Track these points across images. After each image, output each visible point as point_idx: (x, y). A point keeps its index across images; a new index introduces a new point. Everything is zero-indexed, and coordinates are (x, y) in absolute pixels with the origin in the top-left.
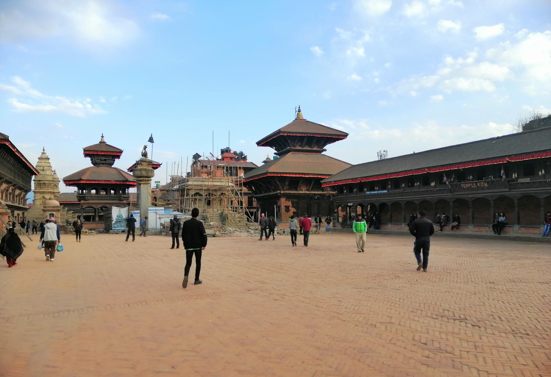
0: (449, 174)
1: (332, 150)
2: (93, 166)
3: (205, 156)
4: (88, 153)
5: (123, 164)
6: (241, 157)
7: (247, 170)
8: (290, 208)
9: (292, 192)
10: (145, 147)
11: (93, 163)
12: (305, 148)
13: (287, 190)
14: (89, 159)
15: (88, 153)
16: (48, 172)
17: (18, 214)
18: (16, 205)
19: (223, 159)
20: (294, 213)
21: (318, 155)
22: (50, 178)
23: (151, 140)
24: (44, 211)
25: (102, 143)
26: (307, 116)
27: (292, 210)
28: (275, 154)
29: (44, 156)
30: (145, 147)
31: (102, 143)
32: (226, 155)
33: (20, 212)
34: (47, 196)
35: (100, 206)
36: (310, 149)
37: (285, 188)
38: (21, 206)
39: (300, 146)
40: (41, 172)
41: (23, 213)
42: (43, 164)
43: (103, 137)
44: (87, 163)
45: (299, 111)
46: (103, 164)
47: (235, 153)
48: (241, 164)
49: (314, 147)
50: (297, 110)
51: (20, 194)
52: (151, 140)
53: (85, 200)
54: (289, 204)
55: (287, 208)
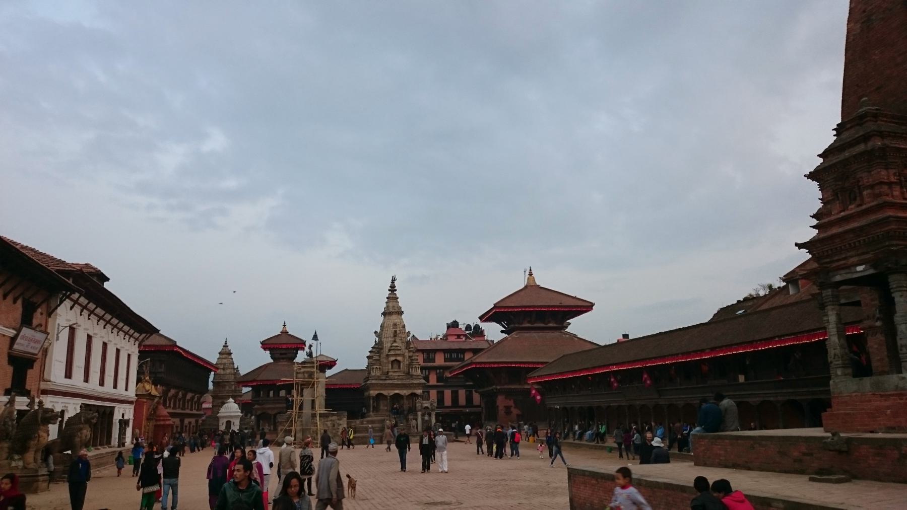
1: (577, 326)
2: (272, 361)
4: (266, 345)
6: (478, 332)
7: (476, 351)
8: (512, 409)
9: (513, 387)
10: (310, 346)
11: (272, 358)
12: (536, 325)
15: (266, 345)
17: (190, 423)
18: (188, 411)
20: (518, 415)
21: (557, 334)
25: (285, 333)
27: (515, 411)
28: (502, 332)
31: (285, 333)
32: (453, 331)
33: (193, 420)
35: (276, 411)
36: (542, 325)
38: (195, 412)
39: (529, 322)
41: (197, 421)
44: (266, 358)
45: (531, 274)
46: (283, 359)
47: (468, 327)
48: (474, 343)
50: (527, 273)
51: (193, 398)
53: (258, 404)
54: (511, 403)
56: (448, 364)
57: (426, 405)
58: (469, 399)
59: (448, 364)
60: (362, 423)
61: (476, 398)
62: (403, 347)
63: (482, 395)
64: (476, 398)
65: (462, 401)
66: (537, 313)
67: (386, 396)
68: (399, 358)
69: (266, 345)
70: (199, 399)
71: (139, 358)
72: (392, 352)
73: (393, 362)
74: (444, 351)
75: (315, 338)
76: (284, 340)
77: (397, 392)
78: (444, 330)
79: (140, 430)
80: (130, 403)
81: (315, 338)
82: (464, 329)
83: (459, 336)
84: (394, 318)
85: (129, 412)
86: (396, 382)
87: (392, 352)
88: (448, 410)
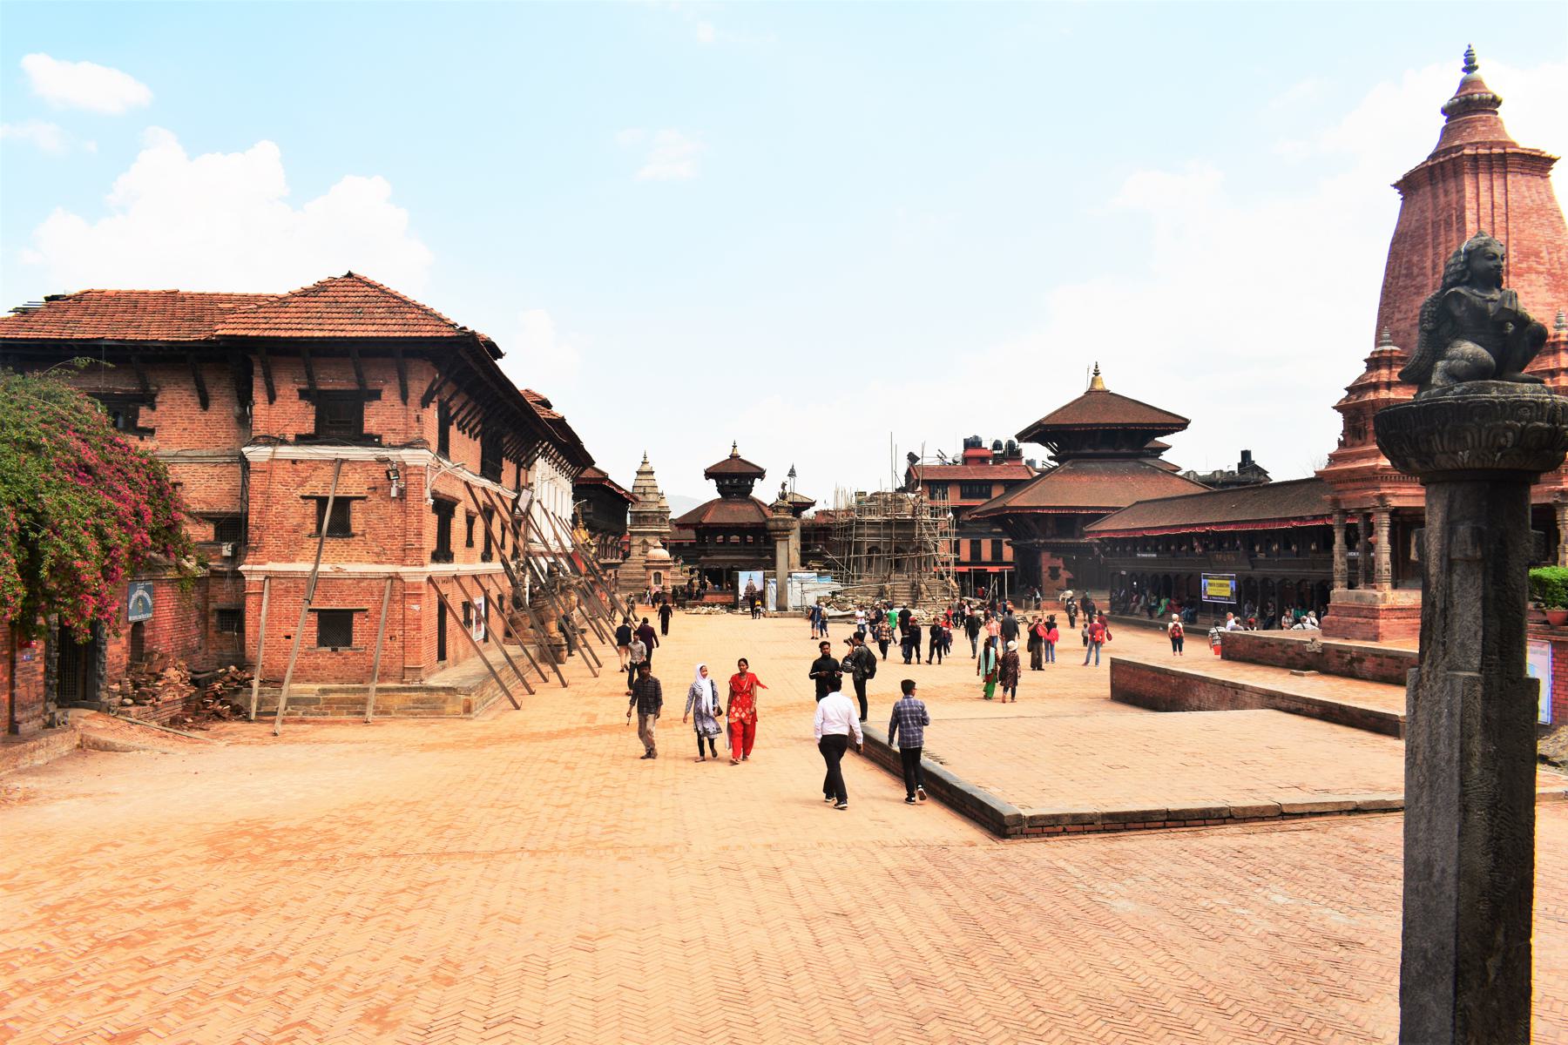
0: (1200, 536)
3: (929, 459)
5: (765, 492)
6: (1013, 453)
10: (784, 485)
13: (1053, 536)
14: (713, 482)
16: (651, 498)
18: (609, 560)
19: (966, 460)
22: (655, 508)
23: (792, 473)
24: (647, 568)
25: (734, 457)
26: (1113, 383)
27: (1065, 575)
28: (1050, 458)
29: (646, 468)
30: (784, 485)
32: (972, 452)
34: (650, 540)
35: (728, 565)
36: (1111, 451)
37: (1049, 533)
40: (641, 498)
42: (644, 483)
44: (710, 491)
45: (1097, 373)
47: (997, 445)
49: (1121, 446)
52: (792, 473)
54: (1060, 563)
55: (1054, 573)
56: (966, 502)
58: (997, 557)
59: (966, 502)
61: (1008, 553)
63: (1016, 550)
64: (1008, 553)
65: (986, 554)
66: (1107, 433)
69: (709, 474)
71: (575, 498)
74: (961, 483)
76: (736, 469)
78: (960, 450)
82: (990, 447)
83: (983, 460)
88: (965, 569)
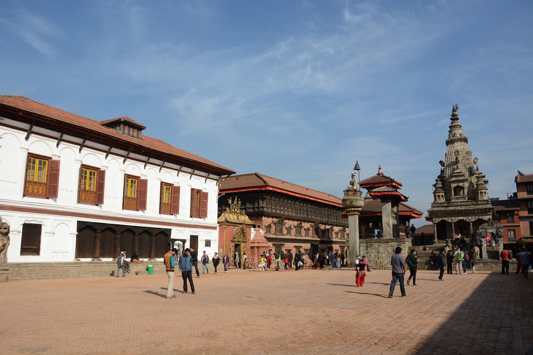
10: (353, 176)
30: (353, 176)
43: (380, 169)
57: (491, 231)
60: (425, 249)
62: (467, 174)
67: (451, 223)
68: (461, 184)
70: (344, 230)
72: (454, 179)
73: (455, 188)
75: (357, 168)
77: (459, 218)
79: (223, 249)
80: (215, 228)
81: (357, 168)
84: (458, 146)
85: (214, 236)
86: (458, 208)
87: (454, 179)
